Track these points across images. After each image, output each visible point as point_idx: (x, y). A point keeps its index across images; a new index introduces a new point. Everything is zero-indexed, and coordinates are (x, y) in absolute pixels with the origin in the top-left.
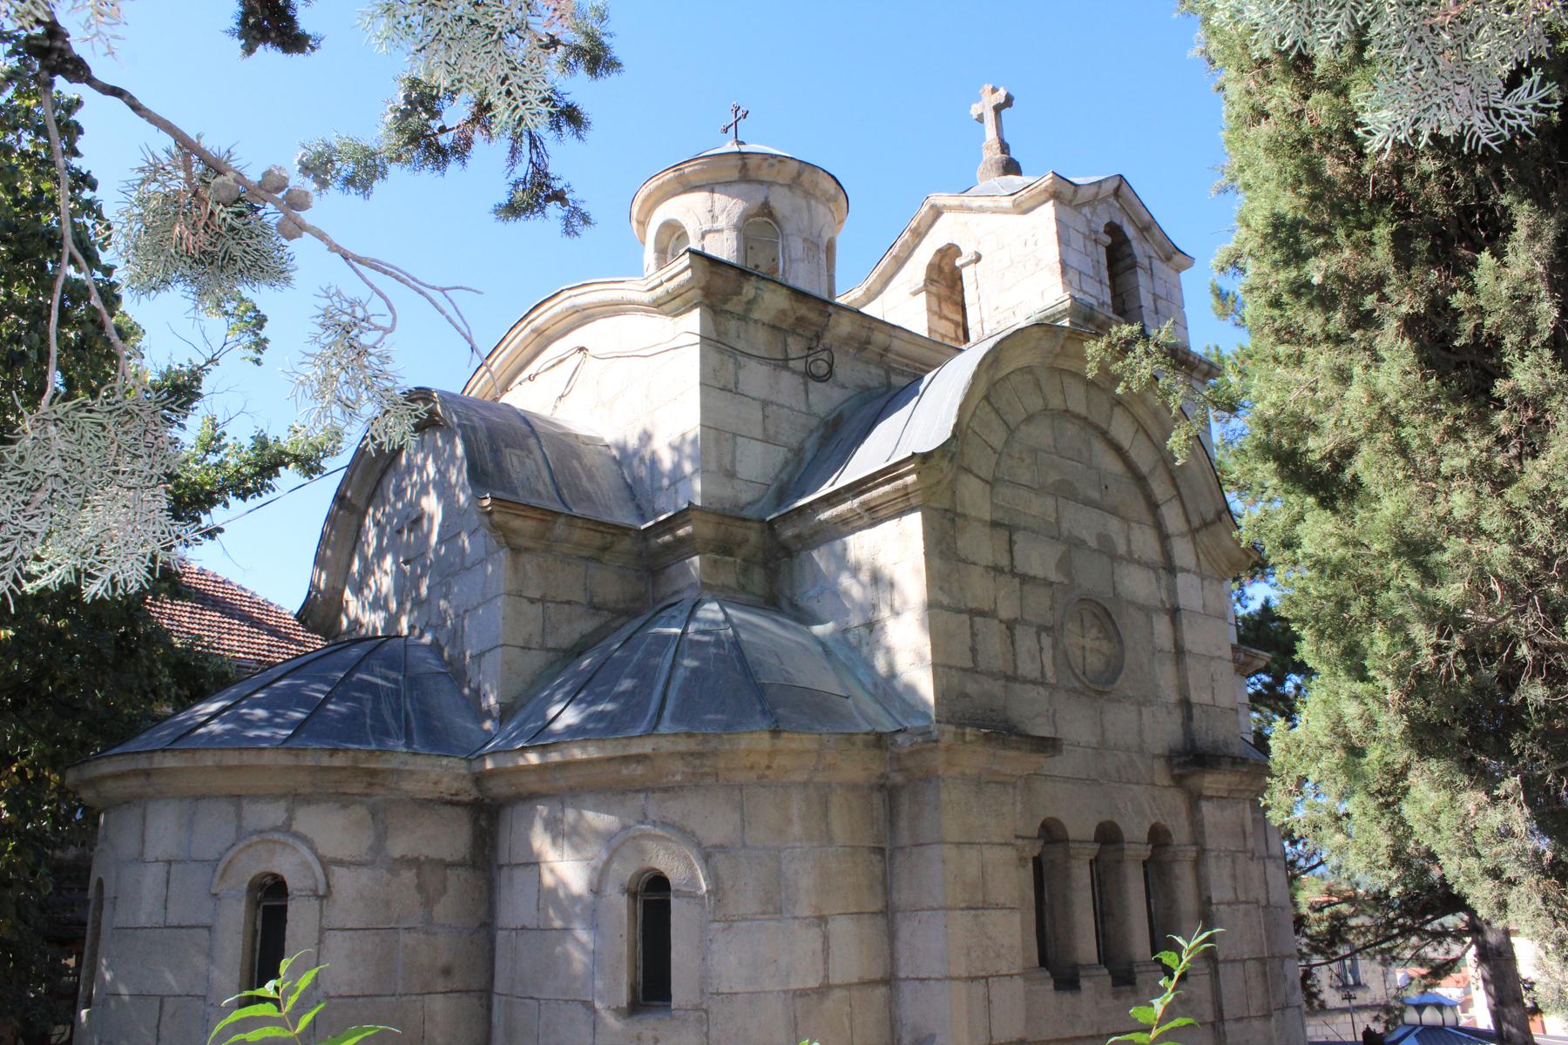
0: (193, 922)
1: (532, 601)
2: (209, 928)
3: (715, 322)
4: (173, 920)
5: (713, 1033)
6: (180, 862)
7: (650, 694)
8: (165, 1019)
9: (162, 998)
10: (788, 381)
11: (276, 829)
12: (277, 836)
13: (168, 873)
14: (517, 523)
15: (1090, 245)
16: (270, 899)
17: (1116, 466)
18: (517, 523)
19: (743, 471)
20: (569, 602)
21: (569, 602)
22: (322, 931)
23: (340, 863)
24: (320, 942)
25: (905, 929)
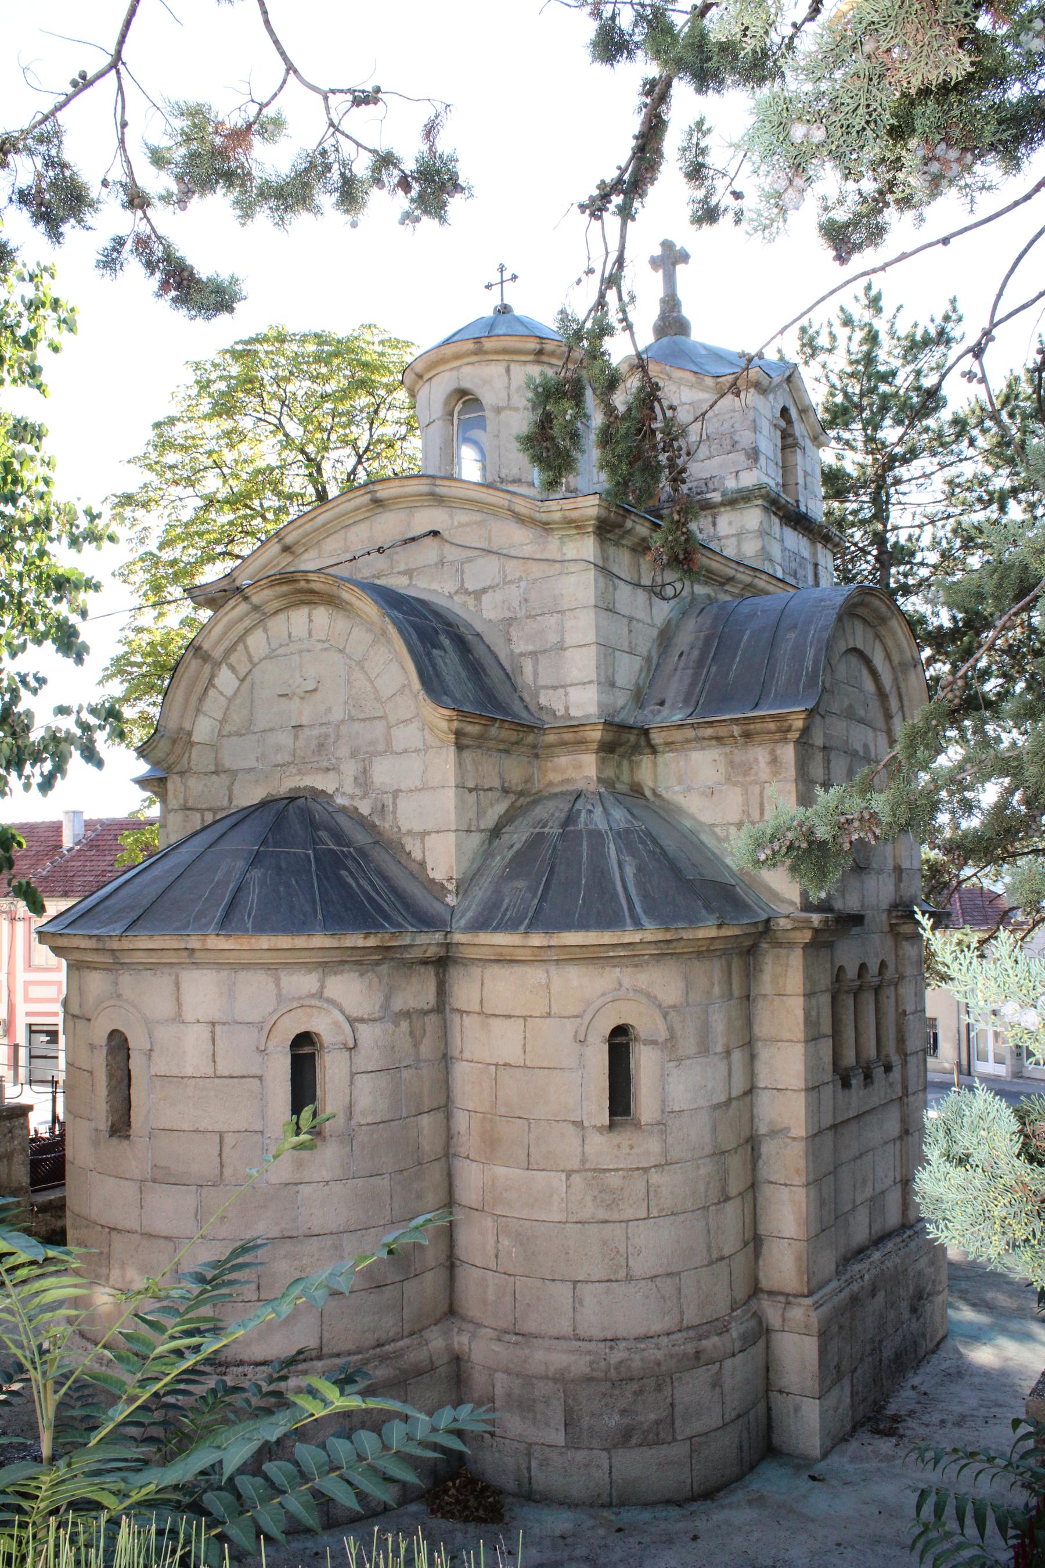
0: (245, 1073)
1: (470, 790)
2: (260, 1078)
3: (603, 550)
4: (222, 1070)
5: (670, 1140)
6: (224, 1024)
7: (615, 888)
8: (226, 1149)
9: (221, 1136)
10: (641, 596)
11: (313, 996)
12: (313, 1002)
13: (213, 1032)
14: (470, 729)
15: (772, 429)
16: (304, 1053)
17: (869, 686)
18: (470, 729)
19: (620, 681)
20: (490, 789)
21: (490, 789)
22: (353, 1075)
23: (362, 1020)
24: (351, 1083)
25: (764, 1053)
